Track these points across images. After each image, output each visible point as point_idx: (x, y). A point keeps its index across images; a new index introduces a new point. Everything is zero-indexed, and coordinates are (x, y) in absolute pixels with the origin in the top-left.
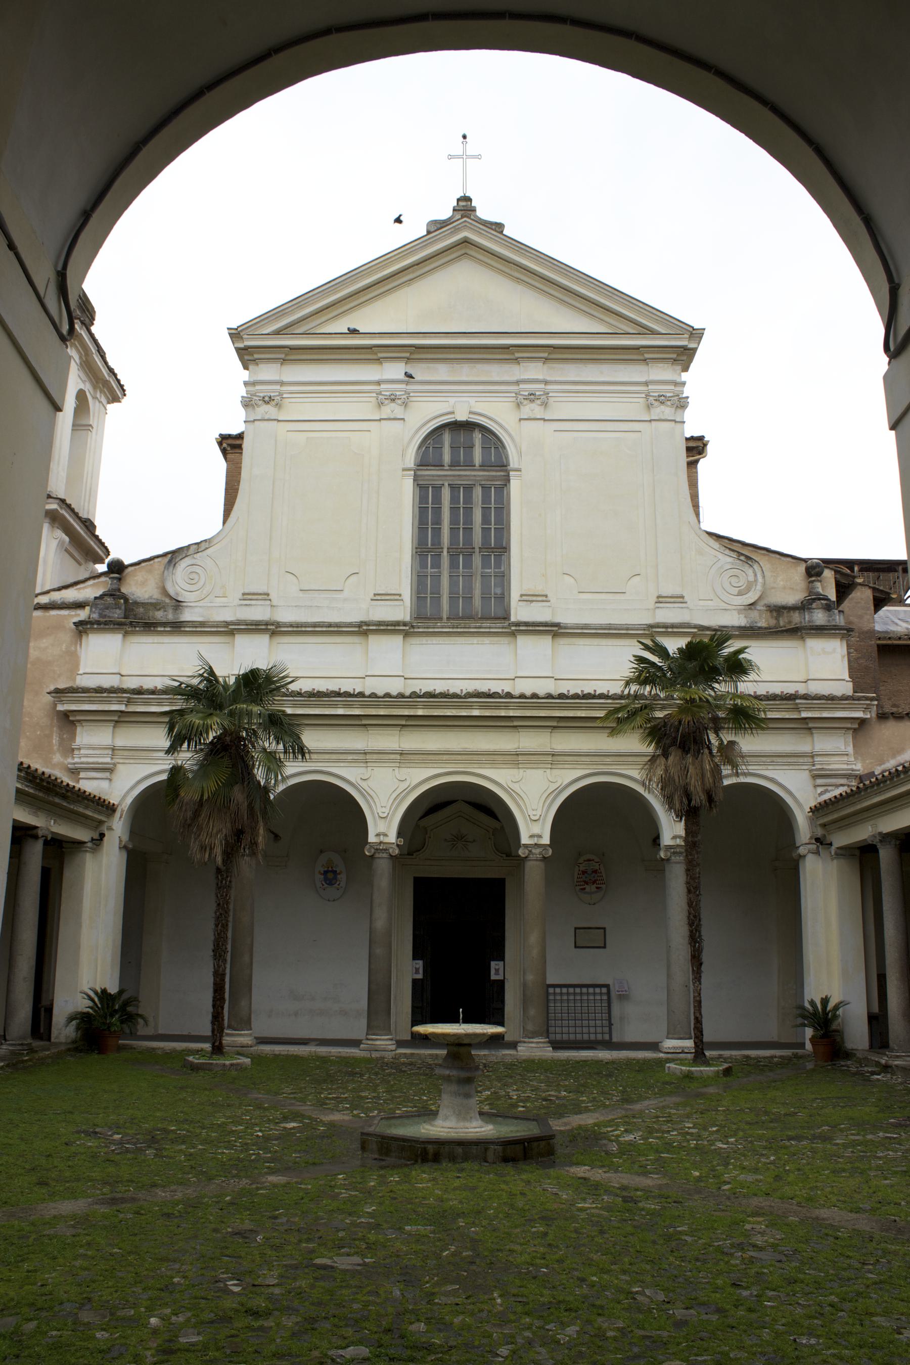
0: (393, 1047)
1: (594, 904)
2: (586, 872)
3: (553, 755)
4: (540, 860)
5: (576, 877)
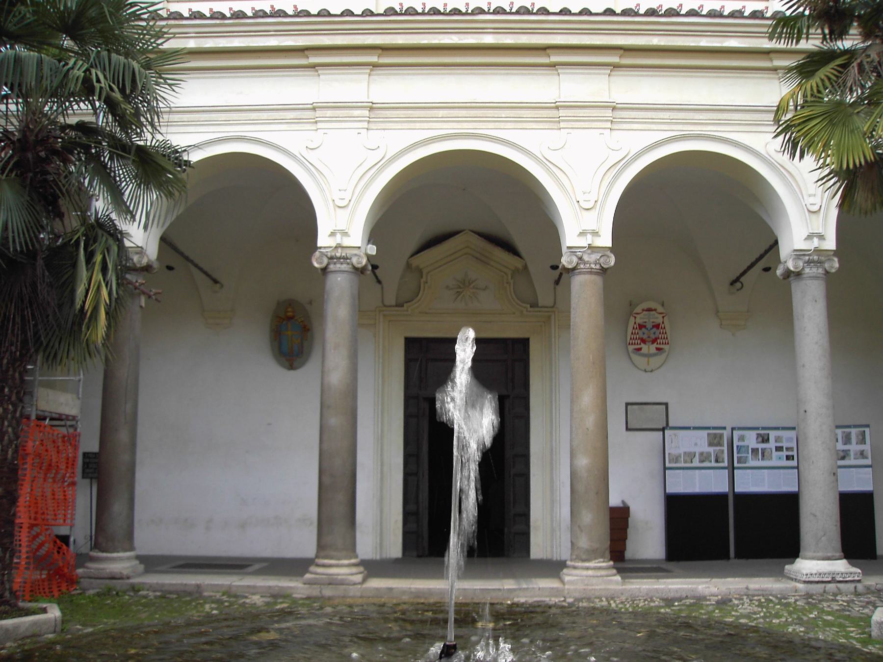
0: (359, 578)
1: (652, 371)
2: (645, 327)
3: (614, 109)
4: (597, 273)
5: (629, 333)
